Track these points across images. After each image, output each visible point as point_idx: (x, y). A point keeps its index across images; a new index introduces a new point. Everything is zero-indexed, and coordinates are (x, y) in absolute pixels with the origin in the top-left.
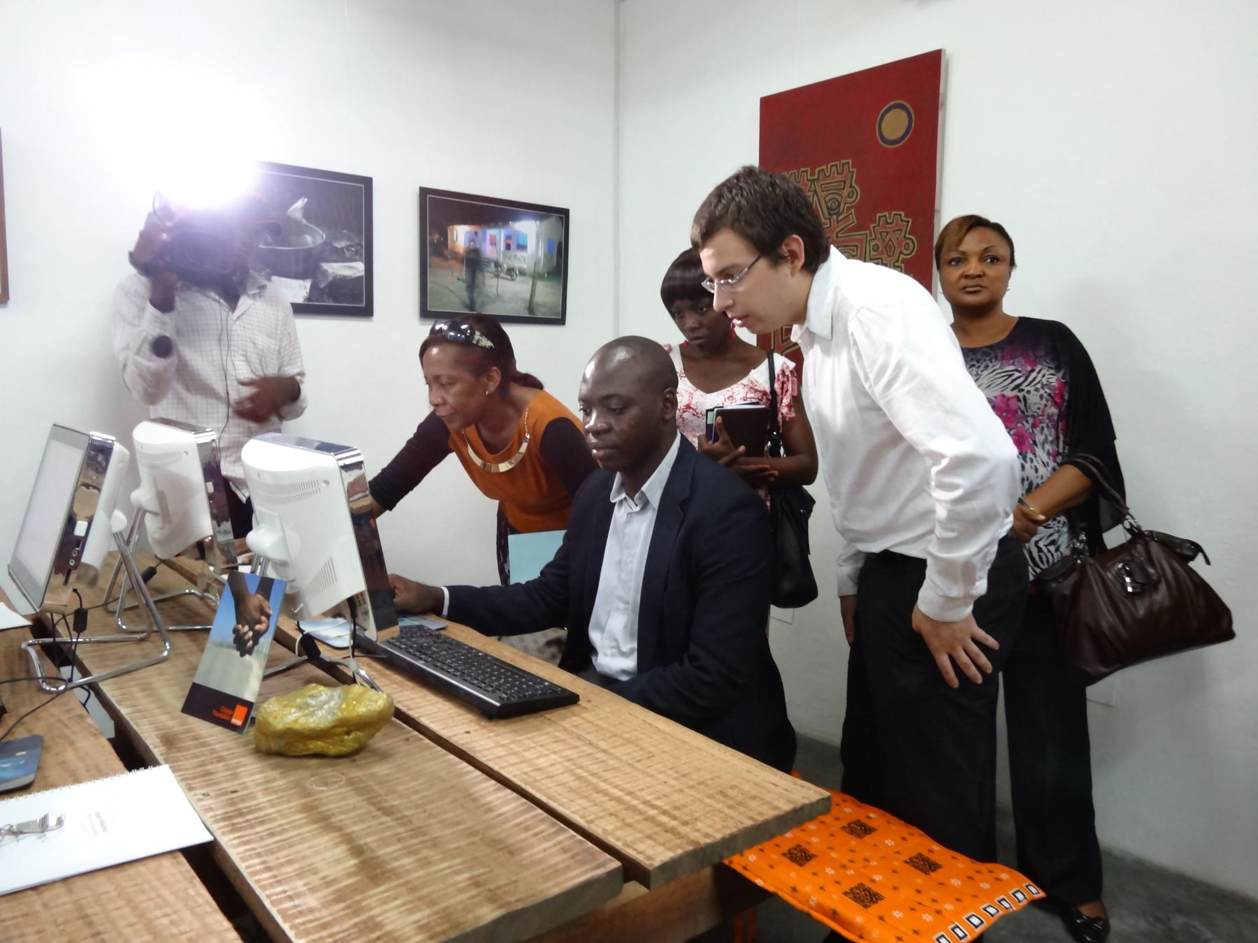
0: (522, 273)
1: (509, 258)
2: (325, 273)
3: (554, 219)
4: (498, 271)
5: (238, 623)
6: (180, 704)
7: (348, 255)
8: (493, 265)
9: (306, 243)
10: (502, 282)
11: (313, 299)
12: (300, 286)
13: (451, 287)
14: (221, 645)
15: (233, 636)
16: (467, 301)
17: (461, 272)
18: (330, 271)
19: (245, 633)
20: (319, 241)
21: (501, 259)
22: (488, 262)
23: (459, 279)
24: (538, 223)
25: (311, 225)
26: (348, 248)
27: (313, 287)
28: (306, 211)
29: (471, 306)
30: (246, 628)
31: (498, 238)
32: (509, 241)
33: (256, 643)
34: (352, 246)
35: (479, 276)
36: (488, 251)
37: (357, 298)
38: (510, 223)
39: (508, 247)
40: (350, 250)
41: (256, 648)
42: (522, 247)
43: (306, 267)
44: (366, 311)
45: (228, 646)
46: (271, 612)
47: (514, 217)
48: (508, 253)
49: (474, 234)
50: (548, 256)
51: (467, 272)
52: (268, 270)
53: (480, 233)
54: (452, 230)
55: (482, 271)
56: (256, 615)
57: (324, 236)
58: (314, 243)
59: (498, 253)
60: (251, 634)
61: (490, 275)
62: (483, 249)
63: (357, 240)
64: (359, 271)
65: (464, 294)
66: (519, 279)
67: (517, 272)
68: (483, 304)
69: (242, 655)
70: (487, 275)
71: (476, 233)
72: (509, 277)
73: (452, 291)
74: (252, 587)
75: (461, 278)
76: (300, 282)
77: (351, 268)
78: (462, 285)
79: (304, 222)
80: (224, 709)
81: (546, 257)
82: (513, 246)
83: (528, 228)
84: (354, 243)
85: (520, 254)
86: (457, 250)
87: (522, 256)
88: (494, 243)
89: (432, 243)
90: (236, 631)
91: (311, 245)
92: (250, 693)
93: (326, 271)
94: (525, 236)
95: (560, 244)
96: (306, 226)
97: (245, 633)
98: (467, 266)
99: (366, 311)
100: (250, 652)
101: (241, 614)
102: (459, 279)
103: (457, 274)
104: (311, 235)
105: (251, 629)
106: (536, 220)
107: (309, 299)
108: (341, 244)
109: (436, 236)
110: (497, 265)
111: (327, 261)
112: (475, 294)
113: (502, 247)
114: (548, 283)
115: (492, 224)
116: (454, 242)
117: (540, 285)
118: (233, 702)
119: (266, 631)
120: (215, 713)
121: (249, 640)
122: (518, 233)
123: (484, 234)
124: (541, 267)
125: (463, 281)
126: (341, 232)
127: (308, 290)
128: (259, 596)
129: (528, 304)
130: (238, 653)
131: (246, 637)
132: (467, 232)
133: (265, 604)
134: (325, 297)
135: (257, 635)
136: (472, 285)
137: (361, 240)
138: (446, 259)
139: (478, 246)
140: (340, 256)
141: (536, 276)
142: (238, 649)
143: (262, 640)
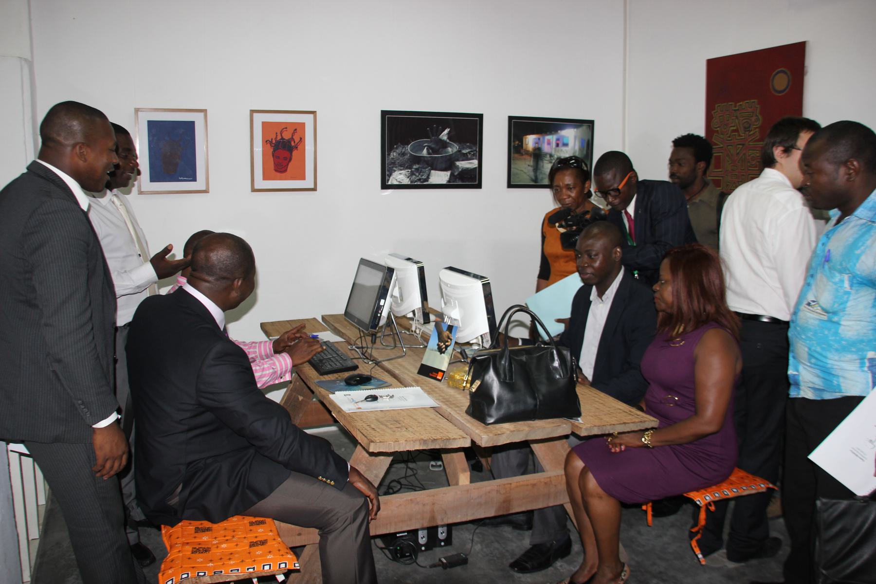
2: (457, 167)
3: (585, 127)
4: (551, 159)
5: (439, 342)
6: (416, 371)
7: (469, 156)
8: (548, 156)
9: (449, 152)
12: (445, 175)
13: (525, 170)
14: (432, 350)
15: (437, 347)
16: (533, 178)
17: (530, 161)
18: (460, 166)
19: (442, 346)
20: (455, 150)
21: (553, 153)
22: (546, 154)
23: (529, 166)
24: (575, 130)
26: (469, 153)
27: (452, 175)
28: (450, 136)
29: (536, 180)
30: (442, 344)
31: (551, 141)
32: (558, 142)
33: (446, 349)
34: (472, 151)
35: (541, 163)
36: (546, 149)
37: (474, 179)
38: (559, 131)
39: (557, 145)
41: (446, 351)
42: (566, 145)
43: (448, 164)
45: (435, 350)
46: (452, 338)
47: (561, 128)
48: (558, 148)
50: (581, 149)
51: (534, 161)
53: (541, 139)
54: (526, 138)
55: (542, 160)
56: (446, 339)
57: (458, 147)
58: (452, 151)
59: (552, 149)
60: (444, 346)
63: (474, 148)
65: (532, 174)
69: (441, 354)
71: (539, 139)
73: (525, 173)
74: (445, 328)
77: (471, 163)
78: (531, 169)
79: (448, 141)
80: (434, 373)
82: (560, 144)
83: (570, 134)
84: (473, 150)
85: (564, 149)
86: (528, 149)
87: (566, 150)
88: (549, 143)
89: (514, 146)
90: (438, 345)
92: (444, 367)
94: (568, 137)
95: (588, 141)
96: (448, 143)
97: (442, 346)
98: (534, 158)
99: (479, 186)
100: (444, 353)
101: (440, 338)
102: (529, 166)
103: (528, 163)
104: (451, 148)
105: (444, 344)
106: (574, 128)
107: (449, 181)
108: (464, 151)
109: (517, 142)
110: (551, 156)
111: (458, 160)
112: (538, 174)
113: (554, 145)
115: (548, 133)
116: (526, 145)
118: (437, 371)
119: (450, 345)
120: (430, 374)
121: (443, 348)
122: (563, 137)
123: (544, 139)
125: (531, 166)
127: (449, 177)
128: (448, 332)
130: (439, 353)
131: (442, 347)
132: (535, 139)
133: (450, 335)
135: (447, 347)
136: (536, 168)
137: (477, 148)
139: (540, 146)
140: (465, 157)
142: (439, 351)
143: (448, 348)
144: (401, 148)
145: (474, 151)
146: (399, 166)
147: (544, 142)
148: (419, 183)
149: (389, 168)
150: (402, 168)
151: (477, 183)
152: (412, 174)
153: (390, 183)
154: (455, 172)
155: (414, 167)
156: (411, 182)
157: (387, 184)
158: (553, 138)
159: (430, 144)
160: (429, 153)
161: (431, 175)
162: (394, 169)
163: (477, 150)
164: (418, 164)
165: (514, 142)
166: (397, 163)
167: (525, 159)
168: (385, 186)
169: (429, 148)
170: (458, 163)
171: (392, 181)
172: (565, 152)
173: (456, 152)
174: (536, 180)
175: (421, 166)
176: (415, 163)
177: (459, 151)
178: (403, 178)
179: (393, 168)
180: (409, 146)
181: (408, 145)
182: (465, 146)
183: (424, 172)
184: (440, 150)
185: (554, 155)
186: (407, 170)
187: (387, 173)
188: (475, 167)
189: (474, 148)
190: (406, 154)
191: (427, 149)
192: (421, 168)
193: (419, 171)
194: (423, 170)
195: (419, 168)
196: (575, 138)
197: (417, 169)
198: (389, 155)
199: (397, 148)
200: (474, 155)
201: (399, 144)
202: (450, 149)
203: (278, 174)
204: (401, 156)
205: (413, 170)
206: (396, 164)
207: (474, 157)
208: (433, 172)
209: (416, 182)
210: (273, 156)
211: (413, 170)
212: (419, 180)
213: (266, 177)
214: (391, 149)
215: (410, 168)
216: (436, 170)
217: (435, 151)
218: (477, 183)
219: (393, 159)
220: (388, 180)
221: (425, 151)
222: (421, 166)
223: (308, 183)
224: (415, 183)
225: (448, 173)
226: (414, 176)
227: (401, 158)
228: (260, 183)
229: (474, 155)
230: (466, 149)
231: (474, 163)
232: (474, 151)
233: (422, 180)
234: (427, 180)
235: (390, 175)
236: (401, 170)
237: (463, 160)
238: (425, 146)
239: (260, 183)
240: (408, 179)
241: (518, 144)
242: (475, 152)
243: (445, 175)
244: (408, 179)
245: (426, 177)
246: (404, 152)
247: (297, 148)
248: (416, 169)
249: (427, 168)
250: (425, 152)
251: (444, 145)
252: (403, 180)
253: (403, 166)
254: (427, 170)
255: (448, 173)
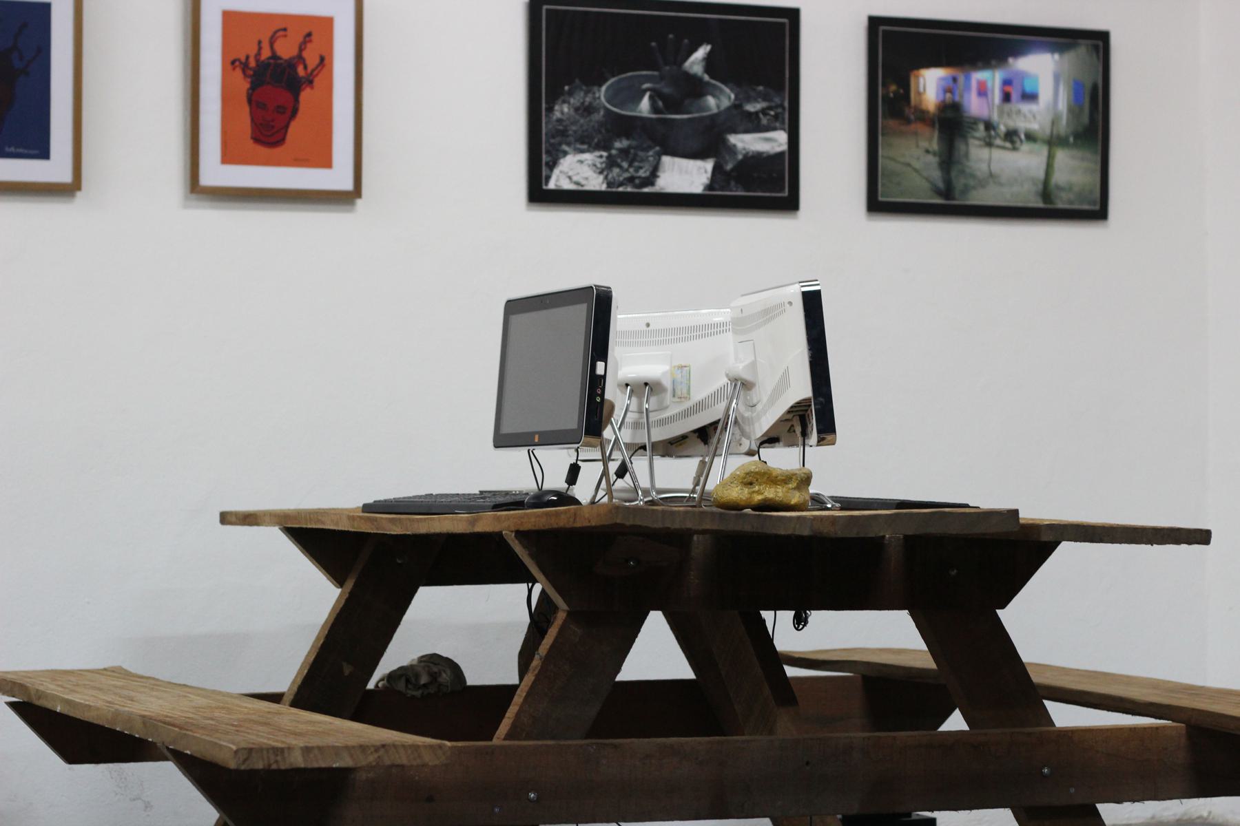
0: (1030, 137)
1: (1009, 115)
2: (732, 150)
7: (764, 121)
8: (981, 127)
9: (708, 108)
10: (997, 154)
11: (717, 186)
12: (700, 168)
13: (917, 165)
16: (941, 185)
17: (931, 141)
18: (740, 145)
20: (726, 103)
21: (995, 117)
22: (975, 121)
23: (927, 151)
25: (713, 82)
26: (764, 111)
27: (717, 169)
29: (947, 192)
31: (989, 84)
32: (1008, 89)
34: (770, 108)
35: (960, 146)
36: (974, 106)
37: (777, 184)
39: (1007, 97)
40: (769, 114)
42: (1031, 97)
44: (790, 204)
48: (1007, 107)
49: (951, 82)
50: (1074, 110)
51: (940, 138)
52: (658, 148)
53: (961, 79)
54: (917, 77)
55: (964, 138)
57: (733, 96)
58: (718, 107)
59: (990, 106)
61: (977, 142)
62: (965, 103)
63: (777, 100)
64: (780, 145)
65: (936, 174)
66: (1026, 147)
67: (1023, 137)
68: (966, 190)
70: (972, 142)
71: (955, 80)
72: (1008, 145)
73: (916, 170)
75: (930, 149)
76: (699, 163)
77: (768, 140)
78: (933, 160)
79: (706, 78)
81: (1070, 110)
84: (773, 104)
85: (1026, 107)
86: (924, 107)
87: (1030, 112)
88: (983, 91)
89: (885, 97)
91: (715, 111)
93: (735, 146)
94: (1035, 78)
95: (1095, 88)
96: (708, 83)
98: (941, 132)
99: (790, 204)
102: (927, 151)
103: (924, 144)
104: (714, 96)
107: (709, 187)
108: (751, 108)
109: (893, 88)
110: (989, 126)
111: (735, 131)
112: (953, 174)
113: (997, 96)
114: (1075, 152)
116: (919, 94)
117: (1062, 156)
122: (1022, 75)
123: (968, 78)
124: (1063, 127)
125: (935, 154)
126: (754, 90)
127: (709, 174)
129: (1040, 187)
132: (943, 79)
134: (733, 183)
136: (949, 160)
137: (783, 101)
138: (908, 121)
139: (957, 98)
140: (754, 124)
141: (1054, 142)
144: (582, 94)
145: (777, 107)
146: (576, 141)
147: (968, 88)
148: (629, 189)
149: (552, 145)
150: (585, 147)
151: (786, 194)
152: (611, 163)
153: (552, 185)
154: (726, 163)
155: (618, 145)
156: (609, 185)
157: (544, 187)
158: (994, 76)
159: (658, 86)
160: (654, 109)
161: (661, 168)
162: (565, 147)
163: (786, 104)
164: (628, 137)
165: (884, 85)
166: (570, 132)
167: (915, 134)
168: (539, 194)
169: (656, 95)
170: (733, 139)
171: (558, 180)
172: (1029, 115)
173: (729, 109)
174: (947, 192)
175: (634, 143)
176: (619, 136)
177: (737, 106)
178: (586, 175)
179: (560, 144)
180: (604, 88)
181: (600, 86)
182: (752, 94)
183: (642, 161)
184: (687, 102)
185: (998, 124)
186: (598, 153)
187: (545, 158)
188: (778, 149)
189: (777, 100)
190: (596, 110)
191: (651, 98)
192: (636, 148)
193: (631, 156)
194: (641, 154)
195: (630, 147)
196: (1057, 78)
197: (624, 152)
198: (550, 110)
199: (570, 93)
200: (776, 117)
201: (577, 81)
202: (711, 101)
203: (263, 151)
204: (582, 116)
205: (614, 152)
206: (568, 136)
207: (778, 125)
208: (666, 160)
209: (621, 184)
210: (250, 101)
211: (614, 152)
212: (631, 180)
213: (229, 156)
214: (555, 95)
215: (606, 147)
216: (675, 153)
217: (673, 104)
218: (786, 194)
219: (559, 121)
220: (548, 178)
221: (645, 105)
222: (634, 143)
223: (338, 177)
224: (621, 189)
225: (709, 165)
226: (616, 171)
227: (582, 121)
228: (215, 173)
229: (776, 117)
230: (756, 100)
231: (777, 141)
232: (777, 107)
233: (637, 181)
234: (651, 179)
235: (552, 165)
236: (582, 151)
237: (747, 131)
238: (645, 91)
239: (215, 173)
240: (601, 178)
241: (895, 93)
242: (779, 110)
243: (700, 168)
244: (601, 178)
245: (648, 174)
246: (590, 103)
247: (311, 82)
248: (621, 151)
249: (650, 148)
250: (645, 105)
251: (694, 88)
252: (587, 179)
253: (586, 142)
254: (651, 153)
255: (709, 165)
